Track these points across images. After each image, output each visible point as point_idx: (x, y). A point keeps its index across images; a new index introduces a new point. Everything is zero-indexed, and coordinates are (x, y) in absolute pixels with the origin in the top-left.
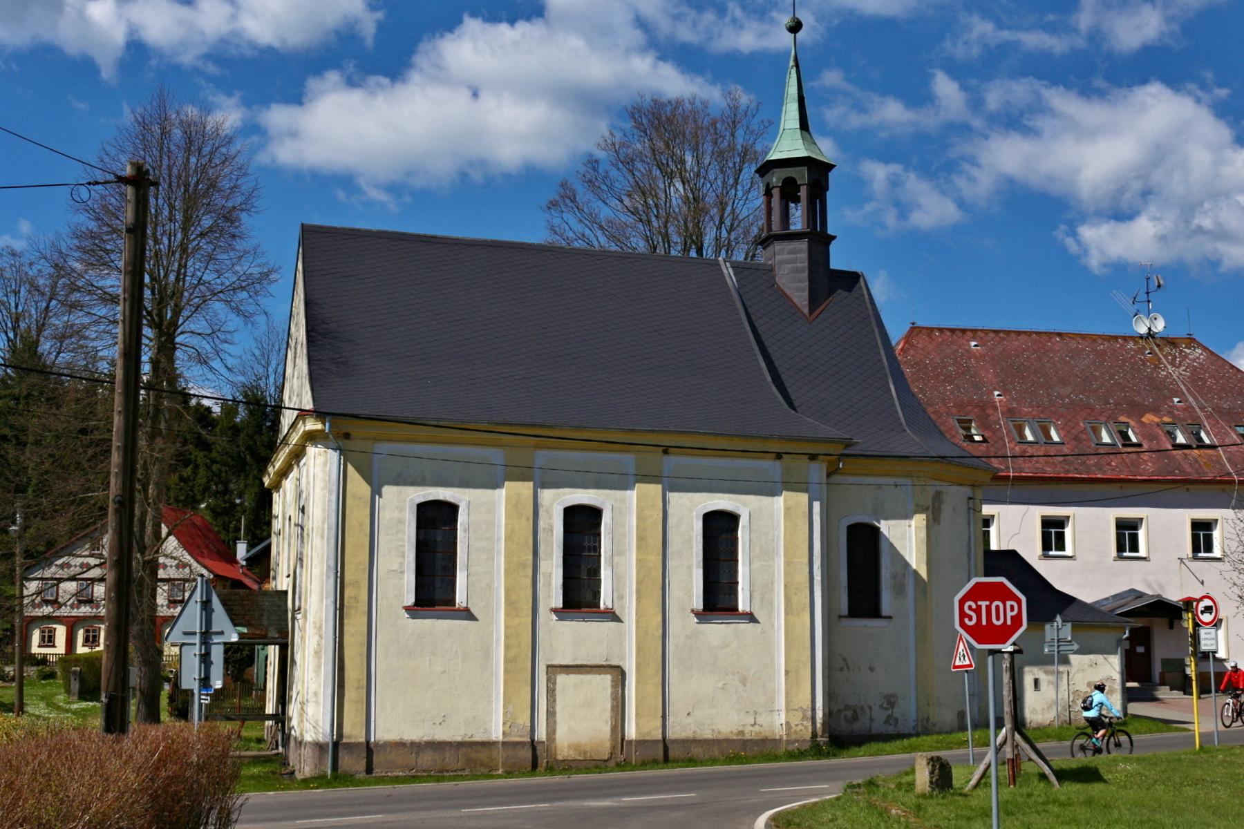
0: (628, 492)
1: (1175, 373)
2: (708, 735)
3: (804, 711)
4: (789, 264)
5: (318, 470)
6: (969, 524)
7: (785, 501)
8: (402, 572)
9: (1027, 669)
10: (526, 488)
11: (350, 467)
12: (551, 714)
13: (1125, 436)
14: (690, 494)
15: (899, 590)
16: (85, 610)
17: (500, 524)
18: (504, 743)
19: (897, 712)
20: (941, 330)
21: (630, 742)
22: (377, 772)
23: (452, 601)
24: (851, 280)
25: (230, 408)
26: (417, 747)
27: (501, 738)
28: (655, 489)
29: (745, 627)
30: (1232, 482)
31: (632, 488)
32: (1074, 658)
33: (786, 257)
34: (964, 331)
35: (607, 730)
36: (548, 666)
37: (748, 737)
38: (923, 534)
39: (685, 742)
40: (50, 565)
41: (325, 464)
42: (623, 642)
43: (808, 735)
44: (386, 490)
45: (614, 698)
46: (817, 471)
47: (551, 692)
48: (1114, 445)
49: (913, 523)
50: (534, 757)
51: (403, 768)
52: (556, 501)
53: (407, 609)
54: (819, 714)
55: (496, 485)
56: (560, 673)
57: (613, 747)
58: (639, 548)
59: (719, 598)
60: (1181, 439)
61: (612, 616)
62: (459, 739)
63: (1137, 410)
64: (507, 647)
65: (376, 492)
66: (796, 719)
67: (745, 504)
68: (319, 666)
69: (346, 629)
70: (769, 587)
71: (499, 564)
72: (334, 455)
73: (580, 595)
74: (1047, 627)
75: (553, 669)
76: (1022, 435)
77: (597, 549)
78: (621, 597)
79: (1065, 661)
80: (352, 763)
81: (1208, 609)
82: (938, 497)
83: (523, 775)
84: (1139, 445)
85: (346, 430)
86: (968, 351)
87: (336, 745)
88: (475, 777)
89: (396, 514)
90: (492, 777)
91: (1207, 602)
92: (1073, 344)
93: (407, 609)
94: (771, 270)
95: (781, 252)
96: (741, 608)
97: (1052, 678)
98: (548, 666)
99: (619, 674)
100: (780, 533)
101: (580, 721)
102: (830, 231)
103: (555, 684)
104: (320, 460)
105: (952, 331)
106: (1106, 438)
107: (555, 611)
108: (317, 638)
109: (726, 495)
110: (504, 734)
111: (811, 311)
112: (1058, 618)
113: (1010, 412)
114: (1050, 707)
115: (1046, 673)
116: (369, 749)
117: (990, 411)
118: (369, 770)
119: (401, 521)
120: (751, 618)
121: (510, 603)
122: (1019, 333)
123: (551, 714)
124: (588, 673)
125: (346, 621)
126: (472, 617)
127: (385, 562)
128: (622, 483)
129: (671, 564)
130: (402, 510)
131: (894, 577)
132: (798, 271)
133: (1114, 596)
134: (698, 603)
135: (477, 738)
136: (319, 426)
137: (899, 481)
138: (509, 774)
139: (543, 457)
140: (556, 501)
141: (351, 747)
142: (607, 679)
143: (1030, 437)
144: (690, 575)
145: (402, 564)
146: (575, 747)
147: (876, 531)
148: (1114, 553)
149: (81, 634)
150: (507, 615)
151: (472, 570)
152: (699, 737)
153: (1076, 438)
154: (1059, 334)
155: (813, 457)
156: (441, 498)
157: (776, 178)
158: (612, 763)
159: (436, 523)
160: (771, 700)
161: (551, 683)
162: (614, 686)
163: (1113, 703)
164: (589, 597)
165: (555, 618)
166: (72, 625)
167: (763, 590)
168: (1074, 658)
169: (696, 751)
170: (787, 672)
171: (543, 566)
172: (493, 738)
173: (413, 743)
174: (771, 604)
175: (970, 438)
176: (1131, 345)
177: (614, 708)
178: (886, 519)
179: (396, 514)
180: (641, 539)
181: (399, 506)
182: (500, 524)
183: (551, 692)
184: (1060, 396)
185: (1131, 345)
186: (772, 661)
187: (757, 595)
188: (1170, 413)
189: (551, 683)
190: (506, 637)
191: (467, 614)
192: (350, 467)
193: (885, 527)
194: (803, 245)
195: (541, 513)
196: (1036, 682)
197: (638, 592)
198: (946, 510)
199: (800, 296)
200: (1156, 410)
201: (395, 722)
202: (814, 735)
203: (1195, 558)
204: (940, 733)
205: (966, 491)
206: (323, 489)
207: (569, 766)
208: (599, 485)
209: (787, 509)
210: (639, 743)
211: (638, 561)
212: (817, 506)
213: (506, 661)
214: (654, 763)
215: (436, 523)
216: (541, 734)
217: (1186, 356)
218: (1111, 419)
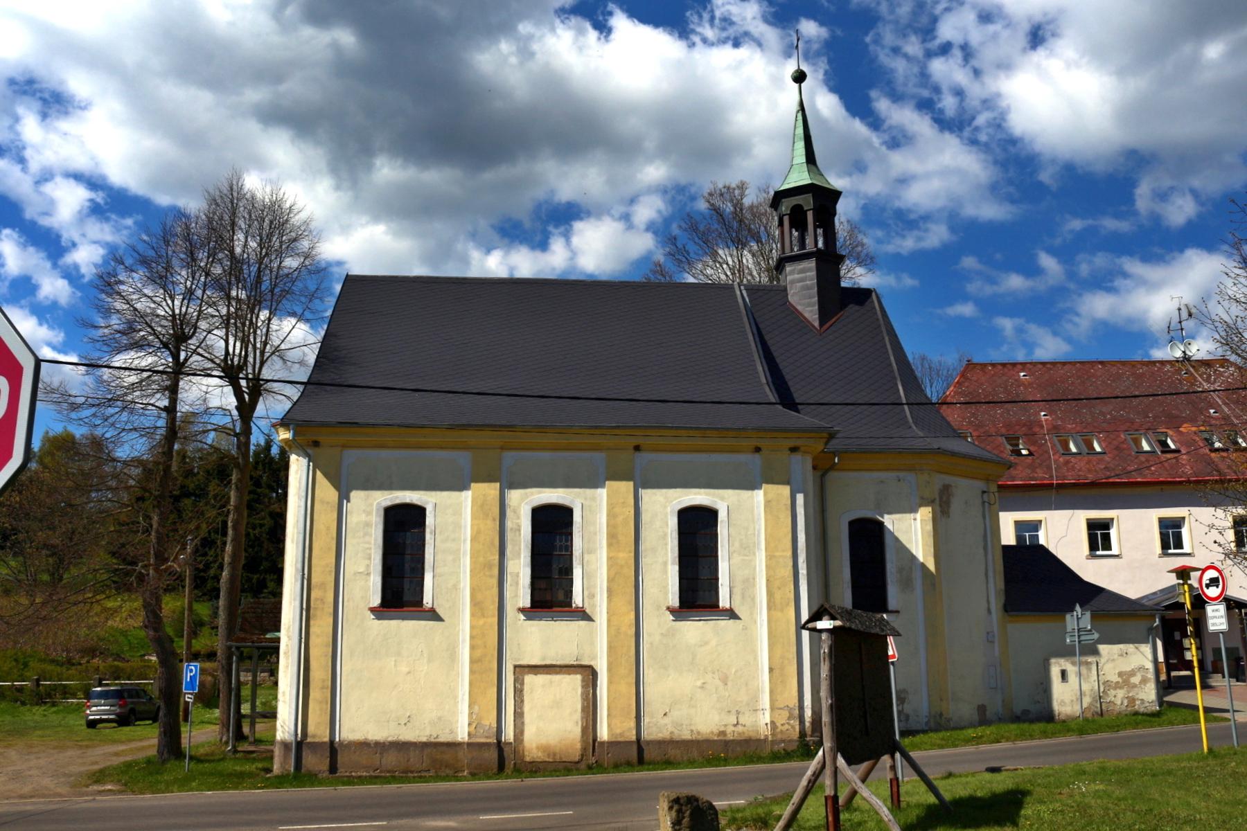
0: (599, 490)
2: (686, 735)
3: (790, 710)
4: (801, 283)
6: (984, 517)
7: (765, 494)
8: (369, 574)
9: (1053, 661)
10: (490, 490)
12: (519, 715)
13: (1164, 444)
14: (664, 491)
15: (906, 584)
18: (469, 744)
20: (993, 365)
21: (602, 743)
22: (342, 772)
23: (420, 602)
24: (862, 296)
26: (381, 747)
27: (466, 739)
31: (603, 486)
32: (1103, 648)
33: (796, 276)
34: (1014, 365)
35: (578, 731)
36: (515, 667)
37: (730, 737)
38: (930, 527)
39: (661, 743)
42: (590, 639)
43: (795, 734)
45: (585, 697)
46: (802, 465)
47: (519, 693)
48: (1153, 452)
49: (918, 516)
50: (499, 758)
51: (367, 768)
52: (523, 502)
53: (372, 610)
55: (462, 486)
56: (529, 673)
57: (584, 749)
58: (610, 545)
59: (698, 593)
60: (1217, 445)
61: (583, 615)
62: (424, 739)
64: (472, 648)
65: (344, 496)
66: (782, 718)
67: (722, 499)
69: (312, 630)
70: (750, 582)
71: (465, 566)
73: (551, 593)
74: (1068, 617)
75: (522, 670)
76: (1067, 448)
77: (569, 548)
78: (592, 596)
79: (1096, 652)
80: (312, 761)
81: (1214, 582)
82: (946, 492)
83: (489, 778)
85: (315, 438)
86: (1018, 380)
87: (300, 745)
88: (438, 778)
89: (363, 517)
90: (458, 779)
91: (1212, 574)
92: (1114, 370)
93: (372, 610)
94: (785, 290)
95: (792, 272)
96: (721, 605)
97: (1075, 669)
98: (515, 667)
99: (590, 674)
100: (759, 527)
101: (548, 720)
103: (522, 684)
105: (1004, 365)
106: (1146, 447)
107: (522, 610)
109: (703, 491)
110: (469, 734)
111: (821, 325)
112: (1078, 608)
113: (1055, 429)
115: (1073, 664)
116: (333, 749)
117: (1037, 429)
118: (333, 769)
119: (368, 524)
120: (731, 614)
121: (475, 603)
122: (1064, 364)
123: (519, 715)
124: (557, 673)
125: (312, 622)
126: (437, 618)
128: (593, 482)
129: (645, 561)
131: (900, 570)
132: (808, 288)
133: (1161, 591)
134: (674, 601)
135: (442, 739)
137: (901, 474)
138: (474, 775)
140: (523, 502)
141: (315, 746)
142: (574, 682)
143: (1073, 449)
144: (665, 572)
145: (368, 566)
146: (545, 749)
147: (881, 524)
148: (1159, 550)
150: (473, 615)
151: (438, 571)
152: (676, 737)
153: (1117, 448)
154: (1101, 363)
155: (794, 450)
156: (408, 501)
157: (786, 206)
158: (583, 766)
160: (755, 699)
162: (584, 686)
163: (1148, 694)
164: (561, 596)
165: (523, 617)
168: (1101, 647)
169: (673, 753)
170: (771, 670)
172: (459, 739)
173: (377, 744)
174: (753, 599)
175: (1018, 453)
176: (1168, 367)
177: (584, 709)
178: (890, 513)
179: (363, 517)
180: (612, 537)
183: (519, 693)
184: (1102, 413)
185: (1168, 367)
186: (755, 659)
187: (737, 591)
188: (1205, 423)
190: (472, 637)
191: (433, 615)
192: (318, 473)
193: (890, 521)
194: (812, 264)
195: (509, 513)
196: (1064, 674)
197: (609, 590)
198: (956, 505)
199: (809, 310)
200: (1192, 420)
201: (358, 723)
202: (803, 734)
204: (947, 729)
205: (980, 485)
207: (535, 768)
209: (768, 503)
210: (612, 744)
211: (609, 558)
212: (800, 498)
213: (472, 661)
214: (629, 765)
216: (509, 734)
217: (1221, 374)
218: (1149, 430)
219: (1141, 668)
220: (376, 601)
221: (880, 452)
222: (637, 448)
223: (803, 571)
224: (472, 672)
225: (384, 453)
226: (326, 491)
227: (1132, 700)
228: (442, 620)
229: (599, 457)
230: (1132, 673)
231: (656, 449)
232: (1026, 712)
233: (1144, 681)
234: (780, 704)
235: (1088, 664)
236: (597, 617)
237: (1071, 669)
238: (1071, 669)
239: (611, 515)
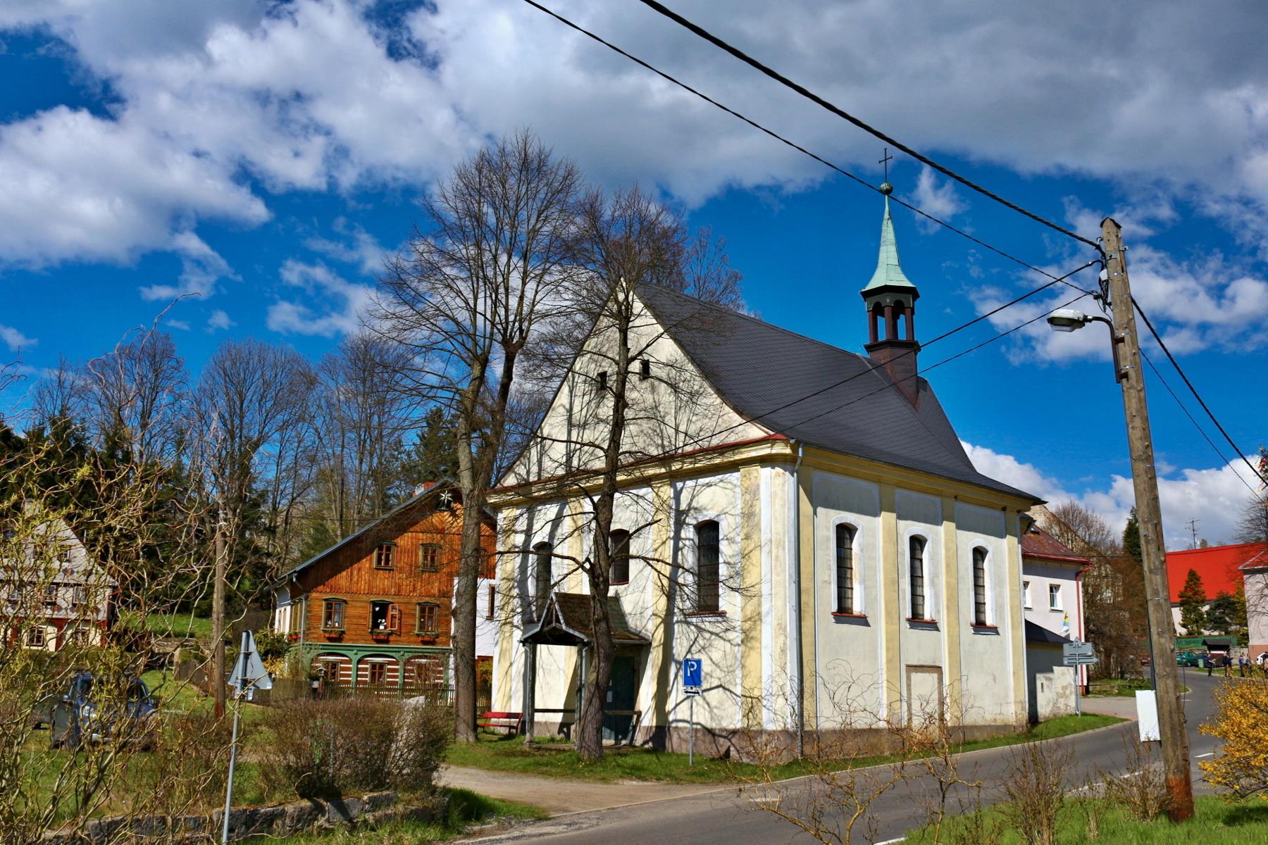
9: (1038, 676)
29: (994, 638)
55: (876, 514)
58: (947, 572)
64: (888, 649)
75: (913, 668)
78: (938, 612)
99: (938, 669)
108: (782, 638)
136: (788, 451)
160: (1007, 696)
161: (909, 678)
189: (909, 678)
190: (887, 641)
206: (783, 506)
211: (948, 583)
225: (835, 478)
227: (1066, 705)
237: (1045, 683)
238: (1045, 683)
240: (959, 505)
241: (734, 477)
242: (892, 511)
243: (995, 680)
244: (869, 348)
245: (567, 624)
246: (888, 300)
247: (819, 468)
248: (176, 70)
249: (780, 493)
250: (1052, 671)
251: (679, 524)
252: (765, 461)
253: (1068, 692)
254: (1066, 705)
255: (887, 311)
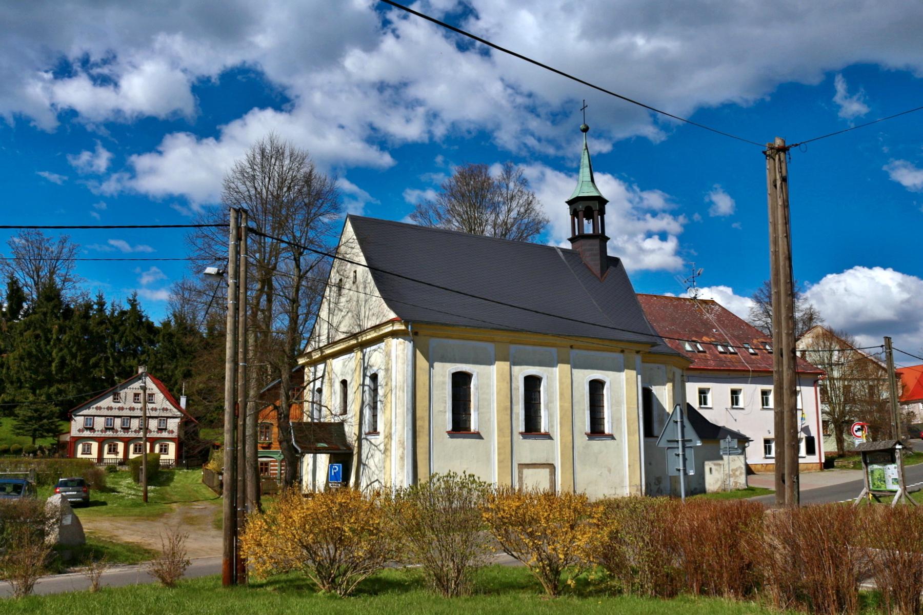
1: (711, 317)
5: (399, 352)
9: (706, 463)
10: (505, 365)
11: (418, 352)
16: (109, 434)
17: (493, 383)
19: (662, 486)
23: (468, 429)
25: (166, 324)
28: (567, 367)
29: (609, 442)
30: (749, 371)
31: (556, 366)
36: (519, 464)
38: (671, 394)
40: (89, 408)
41: (404, 350)
42: (554, 451)
44: (436, 364)
52: (522, 372)
53: (448, 433)
54: (644, 488)
55: (491, 363)
58: (561, 399)
63: (700, 335)
64: (499, 454)
65: (431, 366)
68: (403, 466)
69: (418, 444)
72: (409, 346)
75: (522, 466)
78: (552, 426)
84: (704, 352)
89: (441, 379)
93: (448, 433)
96: (607, 431)
98: (519, 464)
99: (552, 467)
102: (606, 234)
104: (401, 347)
108: (401, 449)
114: (716, 482)
115: (715, 465)
119: (444, 383)
120: (611, 437)
127: (436, 407)
128: (551, 364)
130: (444, 376)
136: (403, 327)
139: (513, 348)
140: (522, 372)
144: (584, 413)
145: (445, 407)
149: (106, 447)
150: (499, 436)
155: (638, 352)
156: (464, 370)
159: (461, 382)
160: (622, 481)
161: (520, 473)
162: (551, 475)
166: (101, 441)
167: (616, 421)
171: (515, 408)
180: (561, 394)
181: (444, 372)
182: (493, 383)
185: (688, 303)
188: (714, 337)
190: (499, 449)
191: (477, 435)
192: (418, 352)
196: (711, 469)
200: (707, 335)
203: (733, 408)
206: (404, 363)
208: (540, 365)
209: (627, 379)
211: (561, 406)
212: (639, 377)
213: (499, 462)
215: (461, 382)
219: (740, 467)
220: (449, 427)
221: (453, 326)
222: (571, 347)
223: (641, 416)
224: (499, 468)
225: (451, 341)
226: (422, 362)
227: (736, 483)
228: (482, 438)
229: (554, 350)
230: (736, 470)
231: (579, 348)
232: (696, 489)
233: (741, 474)
234: (633, 484)
235: (720, 465)
236: (555, 438)
237: (714, 467)
238: (714, 467)
239: (561, 383)
240: (574, 352)
241: (382, 345)
242: (505, 360)
243: (610, 471)
244: (572, 240)
245: (296, 441)
246: (581, 206)
247: (432, 336)
248: (321, 78)
249: (401, 355)
250: (722, 459)
251: (365, 376)
252: (394, 334)
253: (738, 473)
254: (736, 483)
255: (581, 214)
